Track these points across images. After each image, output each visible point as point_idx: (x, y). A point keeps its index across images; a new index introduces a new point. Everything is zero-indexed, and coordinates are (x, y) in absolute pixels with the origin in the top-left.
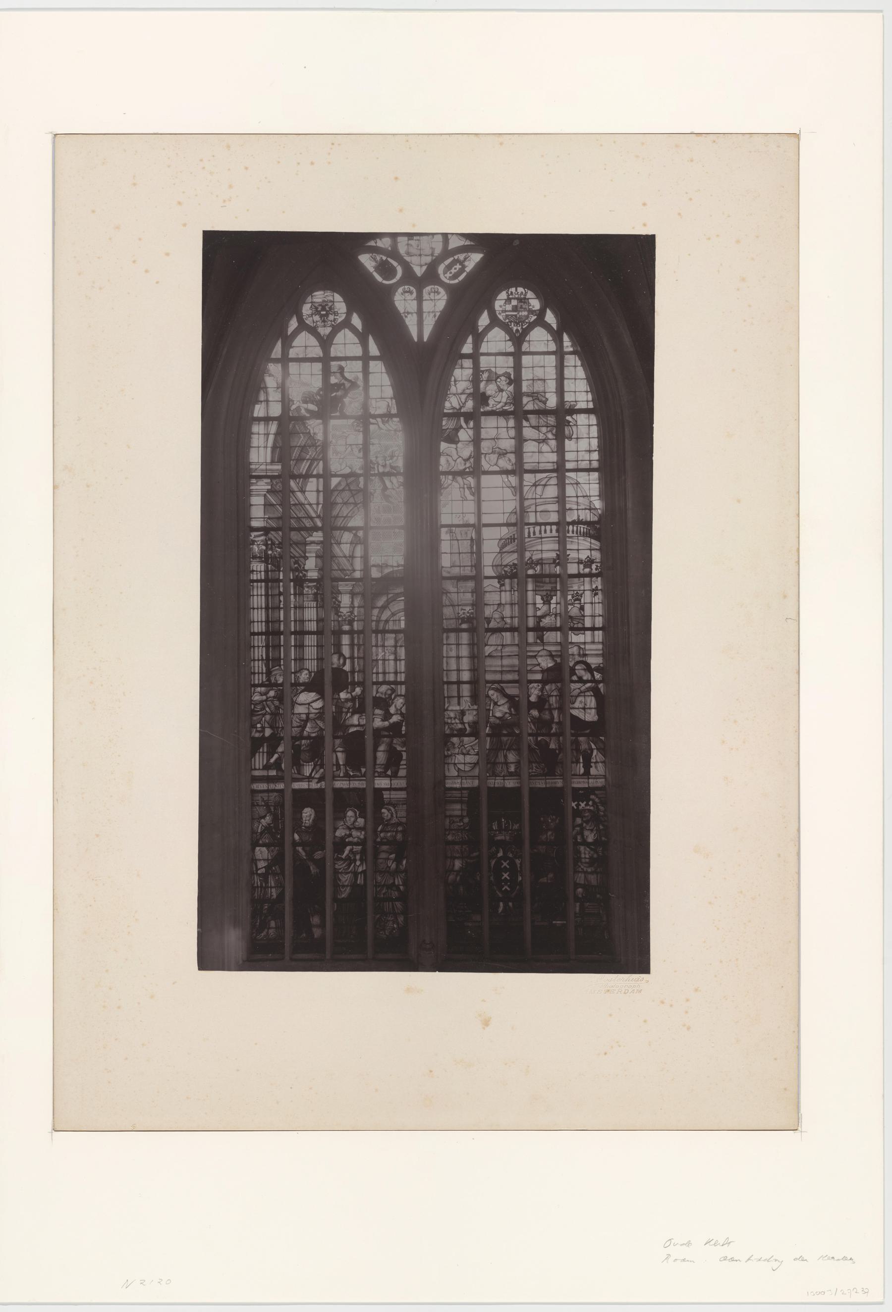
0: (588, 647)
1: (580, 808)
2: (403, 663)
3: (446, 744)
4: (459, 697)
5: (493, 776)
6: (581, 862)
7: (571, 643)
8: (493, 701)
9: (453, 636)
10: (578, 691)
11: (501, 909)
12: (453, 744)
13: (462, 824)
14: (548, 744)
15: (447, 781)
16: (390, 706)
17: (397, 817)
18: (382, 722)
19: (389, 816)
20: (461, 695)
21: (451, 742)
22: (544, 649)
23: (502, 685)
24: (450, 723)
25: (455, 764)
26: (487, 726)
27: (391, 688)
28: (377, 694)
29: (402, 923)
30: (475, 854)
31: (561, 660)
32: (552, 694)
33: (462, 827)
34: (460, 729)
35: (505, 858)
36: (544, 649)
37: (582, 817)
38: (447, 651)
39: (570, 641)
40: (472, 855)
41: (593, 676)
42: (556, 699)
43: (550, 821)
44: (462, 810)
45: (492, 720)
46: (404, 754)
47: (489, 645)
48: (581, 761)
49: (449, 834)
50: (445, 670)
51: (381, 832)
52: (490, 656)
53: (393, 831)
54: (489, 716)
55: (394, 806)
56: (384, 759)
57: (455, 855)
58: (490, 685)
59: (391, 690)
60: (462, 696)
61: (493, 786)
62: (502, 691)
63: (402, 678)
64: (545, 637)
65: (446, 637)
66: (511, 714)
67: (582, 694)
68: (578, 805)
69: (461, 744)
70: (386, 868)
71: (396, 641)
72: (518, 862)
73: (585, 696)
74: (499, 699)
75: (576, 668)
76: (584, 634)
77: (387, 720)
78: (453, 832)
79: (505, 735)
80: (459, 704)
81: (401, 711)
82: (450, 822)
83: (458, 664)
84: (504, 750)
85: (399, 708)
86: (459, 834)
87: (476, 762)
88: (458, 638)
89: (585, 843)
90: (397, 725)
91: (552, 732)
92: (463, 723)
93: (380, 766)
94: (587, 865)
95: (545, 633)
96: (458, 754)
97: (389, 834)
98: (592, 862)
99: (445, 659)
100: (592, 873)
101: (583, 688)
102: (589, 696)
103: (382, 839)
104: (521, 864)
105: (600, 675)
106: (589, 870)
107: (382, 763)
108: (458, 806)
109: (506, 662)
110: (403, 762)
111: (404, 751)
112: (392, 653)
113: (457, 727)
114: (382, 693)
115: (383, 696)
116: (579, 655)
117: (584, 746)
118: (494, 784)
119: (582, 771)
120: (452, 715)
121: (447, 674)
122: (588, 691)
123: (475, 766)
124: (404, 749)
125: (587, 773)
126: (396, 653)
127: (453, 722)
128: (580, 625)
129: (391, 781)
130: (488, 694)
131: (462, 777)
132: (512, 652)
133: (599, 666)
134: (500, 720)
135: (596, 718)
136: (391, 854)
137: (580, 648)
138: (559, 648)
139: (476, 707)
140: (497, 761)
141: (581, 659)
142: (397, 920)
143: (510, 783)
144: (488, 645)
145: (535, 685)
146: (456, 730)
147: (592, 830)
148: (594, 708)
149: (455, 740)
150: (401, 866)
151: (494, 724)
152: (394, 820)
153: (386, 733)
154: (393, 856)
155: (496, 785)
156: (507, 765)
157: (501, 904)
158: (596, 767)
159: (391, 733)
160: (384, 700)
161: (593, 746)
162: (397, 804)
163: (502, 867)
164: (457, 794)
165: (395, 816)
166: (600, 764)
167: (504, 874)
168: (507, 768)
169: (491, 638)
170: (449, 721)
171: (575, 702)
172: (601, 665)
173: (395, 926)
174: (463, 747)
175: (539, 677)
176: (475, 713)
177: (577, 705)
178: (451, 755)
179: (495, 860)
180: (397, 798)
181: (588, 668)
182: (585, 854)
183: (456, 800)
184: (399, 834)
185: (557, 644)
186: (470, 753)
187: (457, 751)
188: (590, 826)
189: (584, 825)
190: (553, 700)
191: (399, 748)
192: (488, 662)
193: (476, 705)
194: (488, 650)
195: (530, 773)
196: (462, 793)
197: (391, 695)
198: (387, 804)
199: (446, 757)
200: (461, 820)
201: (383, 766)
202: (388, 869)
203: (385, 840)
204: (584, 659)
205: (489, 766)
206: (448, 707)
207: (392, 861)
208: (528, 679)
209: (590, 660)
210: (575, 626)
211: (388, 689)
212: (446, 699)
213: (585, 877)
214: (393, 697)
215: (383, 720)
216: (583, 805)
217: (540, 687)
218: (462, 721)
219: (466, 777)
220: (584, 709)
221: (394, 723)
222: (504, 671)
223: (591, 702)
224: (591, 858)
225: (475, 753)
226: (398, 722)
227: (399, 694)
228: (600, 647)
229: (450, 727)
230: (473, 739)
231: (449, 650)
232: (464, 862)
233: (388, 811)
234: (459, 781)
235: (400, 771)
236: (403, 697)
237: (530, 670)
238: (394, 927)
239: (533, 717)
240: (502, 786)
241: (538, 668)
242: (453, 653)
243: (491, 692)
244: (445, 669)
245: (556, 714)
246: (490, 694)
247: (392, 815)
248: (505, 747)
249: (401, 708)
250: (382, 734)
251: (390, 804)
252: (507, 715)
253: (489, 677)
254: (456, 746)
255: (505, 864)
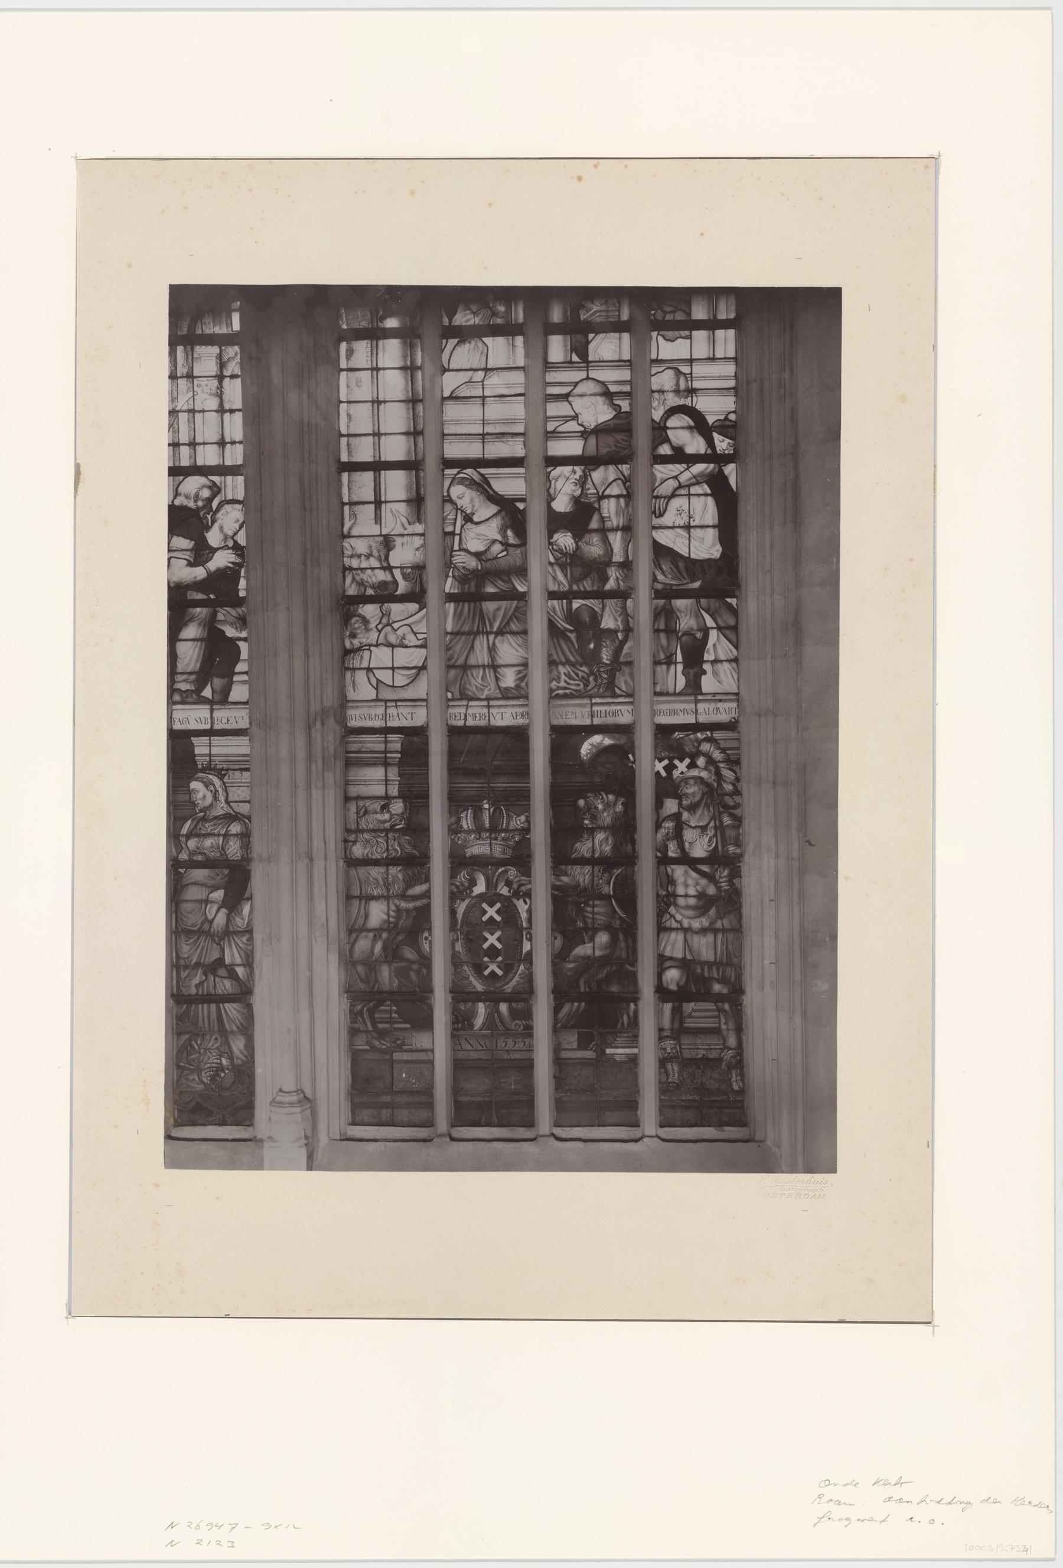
0: (698, 370)
1: (676, 774)
2: (238, 417)
3: (346, 619)
4: (378, 503)
5: (461, 699)
6: (676, 905)
7: (657, 361)
8: (462, 511)
9: (362, 348)
10: (673, 484)
11: (479, 1021)
12: (365, 621)
13: (387, 816)
14: (596, 618)
15: (350, 712)
16: (208, 528)
17: (227, 802)
18: (189, 569)
19: (209, 799)
20: (383, 499)
21: (360, 616)
22: (588, 378)
23: (483, 471)
24: (356, 569)
25: (369, 670)
26: (447, 576)
27: (209, 483)
28: (175, 498)
29: (240, 1056)
30: (418, 889)
31: (630, 404)
32: (607, 493)
33: (387, 825)
34: (383, 584)
35: (491, 898)
36: (588, 378)
37: (678, 797)
38: (348, 386)
39: (654, 356)
40: (410, 892)
41: (710, 443)
42: (618, 503)
43: (600, 807)
44: (386, 781)
45: (460, 559)
46: (244, 647)
47: (453, 370)
48: (679, 658)
49: (355, 842)
50: (344, 436)
51: (189, 836)
52: (453, 397)
53: (219, 835)
54: (453, 551)
55: (221, 774)
56: (194, 660)
57: (369, 891)
58: (455, 471)
59: (210, 488)
60: (386, 502)
61: (461, 723)
62: (483, 487)
63: (235, 456)
64: (591, 347)
65: (347, 351)
66: (506, 545)
67: (683, 492)
68: (669, 769)
69: (384, 621)
70: (203, 923)
71: (222, 365)
72: (522, 907)
73: (689, 495)
74: (477, 505)
75: (670, 423)
76: (690, 337)
77: (202, 563)
78: (366, 836)
79: (493, 597)
80: (378, 519)
81: (236, 542)
82: (358, 813)
83: (376, 417)
84: (488, 633)
85: (230, 533)
86: (380, 840)
87: (420, 665)
88: (374, 352)
89: (686, 860)
90: (227, 577)
91: (608, 587)
92: (389, 568)
93: (184, 677)
94: (690, 913)
95: (591, 336)
96: (377, 645)
97: (208, 842)
98: (704, 903)
99: (343, 407)
100: (703, 931)
101: (685, 477)
102: (699, 495)
103: (192, 853)
104: (529, 911)
105: (727, 441)
106: (696, 925)
107: (189, 670)
108: (378, 773)
109: (495, 410)
110: (241, 667)
111: (245, 640)
112: (211, 394)
113: (374, 580)
114: (187, 497)
115: (191, 504)
116: (677, 391)
117: (686, 623)
118: (465, 719)
119: (681, 682)
120: (361, 546)
121: (348, 445)
122: (698, 483)
123: (418, 674)
124: (244, 634)
125: (694, 687)
126: (222, 393)
127: (364, 565)
128: (680, 316)
129: (212, 711)
130: (449, 495)
131: (386, 701)
132: (508, 386)
133: (726, 419)
134: (480, 560)
135: (716, 552)
136: (215, 888)
137: (678, 373)
138: (625, 374)
139: (419, 528)
140: (472, 661)
141: (682, 402)
142: (230, 1047)
143: (505, 716)
144: (449, 370)
145: (567, 470)
146: (373, 587)
147: (704, 829)
148: (714, 527)
149: (369, 610)
150: (238, 919)
151: (464, 568)
152: (221, 809)
153: (200, 596)
154: (219, 895)
155: (470, 722)
156: (495, 671)
157: (481, 1008)
158: (715, 674)
159: (212, 596)
160: (195, 512)
161: (710, 622)
162: (227, 770)
163: (485, 918)
164: (374, 743)
165: (222, 798)
166: (726, 665)
167: (487, 935)
168: (497, 679)
169: (458, 350)
170: (355, 563)
171: (665, 510)
172: (732, 417)
173: (224, 1062)
174: (389, 628)
175: (574, 447)
176: (418, 541)
177: (668, 519)
178: (359, 649)
179: (467, 901)
180: (227, 756)
181: (700, 425)
182: (686, 886)
183: (371, 758)
184: (231, 843)
185: (619, 363)
186: (406, 642)
187: (373, 637)
188: (699, 819)
189: (685, 815)
190: (610, 508)
191: (230, 632)
192: (452, 411)
193: (419, 521)
194: (450, 382)
195: (551, 690)
196: (386, 742)
197: (209, 500)
198: (203, 770)
199: (347, 652)
200: (385, 808)
201: (193, 677)
202: (206, 927)
203: (200, 858)
204: (688, 402)
205: (453, 673)
206: (350, 529)
207: (215, 907)
208: (550, 453)
209: (704, 404)
210: (668, 317)
211: (204, 486)
212: (346, 508)
213: (686, 940)
214: (215, 504)
215: (190, 564)
216: (682, 766)
217: (577, 476)
218: (385, 564)
219: (396, 701)
220: (688, 527)
221: (218, 570)
222: (488, 434)
223: (705, 510)
224: (701, 896)
225: (419, 643)
226: (228, 567)
227: (229, 497)
228: (730, 369)
229: (358, 578)
230: (413, 607)
231: (353, 385)
232: (393, 907)
233: (207, 787)
234: (380, 711)
235: (234, 687)
236: (239, 507)
237: (554, 432)
238: (221, 1063)
239: (560, 551)
240: (483, 723)
241: (572, 426)
242: (365, 392)
243: (457, 491)
244: (344, 431)
245: (616, 540)
246: (454, 497)
247: (215, 798)
248: (491, 626)
249: (236, 534)
250: (189, 598)
251: (209, 768)
252: (497, 548)
253: (454, 450)
254: (372, 625)
255: (491, 912)
